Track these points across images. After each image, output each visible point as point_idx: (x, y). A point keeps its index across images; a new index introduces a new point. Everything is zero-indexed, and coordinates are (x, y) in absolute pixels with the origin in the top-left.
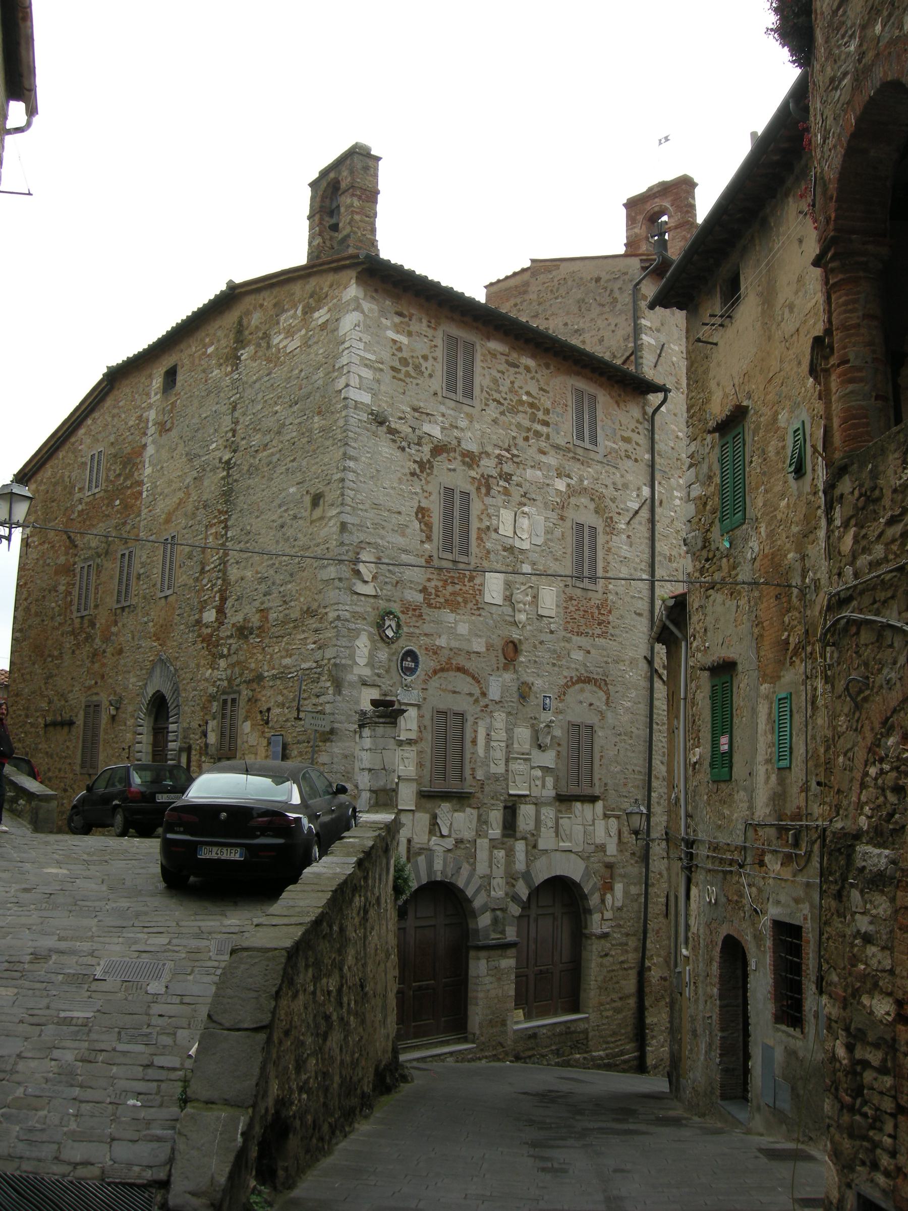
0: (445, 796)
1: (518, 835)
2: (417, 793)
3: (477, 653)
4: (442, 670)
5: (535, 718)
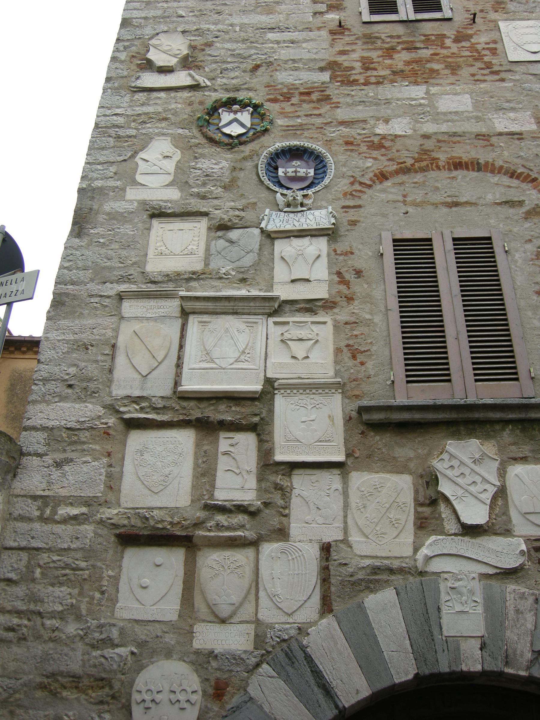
0: (465, 420)
2: (348, 420)
3: (512, 134)
4: (405, 170)
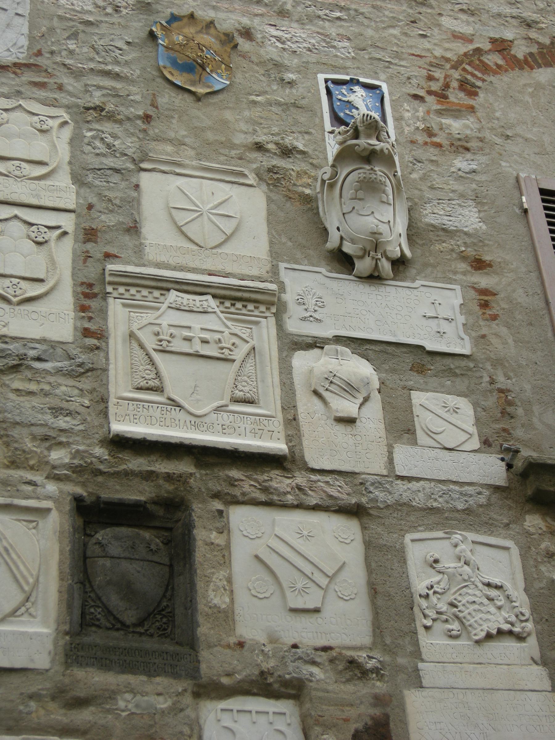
1: (213, 662)
5: (287, 152)
